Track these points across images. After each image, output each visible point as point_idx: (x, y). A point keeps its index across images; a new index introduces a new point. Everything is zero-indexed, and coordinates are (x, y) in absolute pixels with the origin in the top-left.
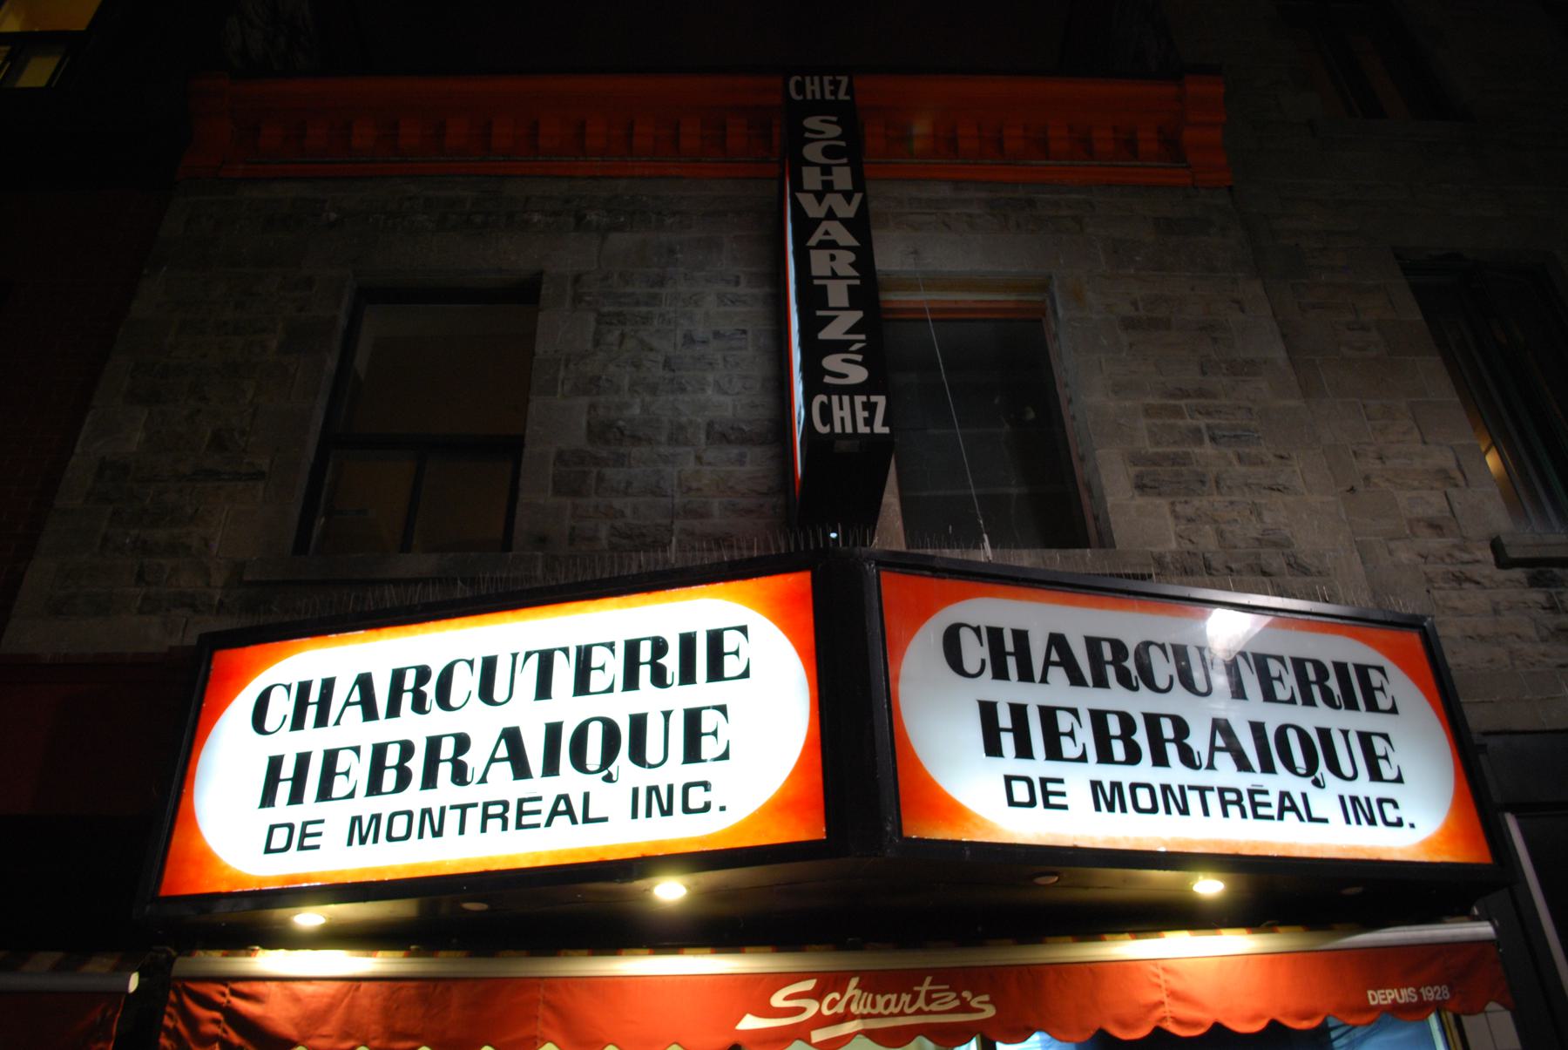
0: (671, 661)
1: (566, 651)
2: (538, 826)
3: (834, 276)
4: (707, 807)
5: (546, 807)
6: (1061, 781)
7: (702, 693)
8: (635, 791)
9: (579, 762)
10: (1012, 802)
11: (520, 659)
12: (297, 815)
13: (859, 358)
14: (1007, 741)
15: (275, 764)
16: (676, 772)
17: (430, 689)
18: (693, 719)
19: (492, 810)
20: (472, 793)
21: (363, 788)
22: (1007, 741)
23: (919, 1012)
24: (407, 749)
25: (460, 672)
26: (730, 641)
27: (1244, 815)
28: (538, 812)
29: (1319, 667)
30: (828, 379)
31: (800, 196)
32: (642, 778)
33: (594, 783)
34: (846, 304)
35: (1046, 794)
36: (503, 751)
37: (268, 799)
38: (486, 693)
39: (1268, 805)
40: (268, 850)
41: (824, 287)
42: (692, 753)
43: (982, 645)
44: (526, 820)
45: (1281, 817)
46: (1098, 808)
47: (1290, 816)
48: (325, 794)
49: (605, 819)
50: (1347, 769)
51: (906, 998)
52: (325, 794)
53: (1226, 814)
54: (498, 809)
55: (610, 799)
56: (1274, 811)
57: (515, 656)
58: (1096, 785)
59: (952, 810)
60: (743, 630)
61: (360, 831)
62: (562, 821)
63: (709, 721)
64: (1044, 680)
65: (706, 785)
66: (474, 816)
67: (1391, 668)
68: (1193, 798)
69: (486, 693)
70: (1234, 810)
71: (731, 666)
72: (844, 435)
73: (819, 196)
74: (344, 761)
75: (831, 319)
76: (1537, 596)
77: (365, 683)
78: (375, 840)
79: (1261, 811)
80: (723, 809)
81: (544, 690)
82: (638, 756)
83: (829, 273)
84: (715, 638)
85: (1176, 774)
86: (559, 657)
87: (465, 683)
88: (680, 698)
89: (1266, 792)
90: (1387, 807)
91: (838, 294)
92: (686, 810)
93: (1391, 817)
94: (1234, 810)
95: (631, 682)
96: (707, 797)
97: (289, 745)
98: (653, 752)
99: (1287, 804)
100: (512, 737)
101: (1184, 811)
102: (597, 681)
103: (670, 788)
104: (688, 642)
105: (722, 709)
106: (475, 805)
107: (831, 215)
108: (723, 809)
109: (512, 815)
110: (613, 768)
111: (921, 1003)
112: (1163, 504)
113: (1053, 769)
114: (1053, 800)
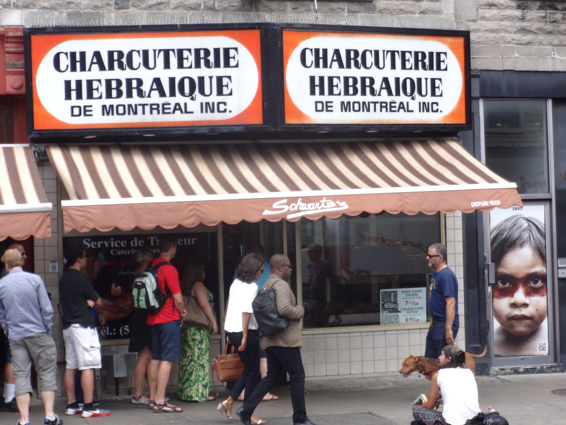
0: (211, 58)
1: (173, 50)
2: (170, 113)
4: (225, 111)
5: (172, 106)
6: (332, 102)
7: (222, 71)
8: (202, 104)
12: (82, 103)
14: (317, 89)
16: (214, 98)
17: (124, 60)
18: (220, 79)
21: (104, 95)
22: (317, 89)
24: (119, 82)
25: (135, 54)
26: (232, 53)
27: (387, 111)
28: (170, 109)
29: (424, 54)
32: (205, 100)
33: (187, 100)
35: (327, 107)
36: (155, 87)
37: (68, 97)
38: (146, 64)
39: (395, 107)
40: (73, 115)
42: (220, 92)
43: (312, 55)
44: (166, 111)
45: (398, 111)
46: (342, 111)
47: (402, 110)
48: (90, 96)
49: (192, 112)
50: (424, 93)
53: (381, 111)
54: (155, 107)
55: (194, 106)
56: (396, 109)
57: (155, 51)
58: (342, 103)
59: (299, 113)
60: (236, 49)
62: (178, 112)
63: (225, 81)
65: (225, 104)
66: (147, 108)
68: (372, 106)
69: (146, 64)
70: (384, 109)
71: (232, 62)
74: (95, 85)
76: (518, 13)
77: (97, 54)
78: (113, 114)
79: (393, 109)
80: (230, 112)
81: (167, 65)
82: (202, 92)
84: (227, 51)
85: (368, 98)
86: (171, 53)
87: (137, 60)
88: (216, 72)
89: (395, 103)
90: (435, 106)
92: (219, 111)
93: (435, 109)
94: (384, 109)
95: (198, 65)
96: (225, 107)
97: (73, 77)
98: (207, 91)
100: (157, 81)
101: (368, 110)
102: (186, 64)
103: (213, 103)
104: (217, 51)
105: (229, 77)
106: (147, 105)
108: (230, 112)
109: (161, 109)
110: (194, 95)
113: (331, 98)
114: (329, 109)
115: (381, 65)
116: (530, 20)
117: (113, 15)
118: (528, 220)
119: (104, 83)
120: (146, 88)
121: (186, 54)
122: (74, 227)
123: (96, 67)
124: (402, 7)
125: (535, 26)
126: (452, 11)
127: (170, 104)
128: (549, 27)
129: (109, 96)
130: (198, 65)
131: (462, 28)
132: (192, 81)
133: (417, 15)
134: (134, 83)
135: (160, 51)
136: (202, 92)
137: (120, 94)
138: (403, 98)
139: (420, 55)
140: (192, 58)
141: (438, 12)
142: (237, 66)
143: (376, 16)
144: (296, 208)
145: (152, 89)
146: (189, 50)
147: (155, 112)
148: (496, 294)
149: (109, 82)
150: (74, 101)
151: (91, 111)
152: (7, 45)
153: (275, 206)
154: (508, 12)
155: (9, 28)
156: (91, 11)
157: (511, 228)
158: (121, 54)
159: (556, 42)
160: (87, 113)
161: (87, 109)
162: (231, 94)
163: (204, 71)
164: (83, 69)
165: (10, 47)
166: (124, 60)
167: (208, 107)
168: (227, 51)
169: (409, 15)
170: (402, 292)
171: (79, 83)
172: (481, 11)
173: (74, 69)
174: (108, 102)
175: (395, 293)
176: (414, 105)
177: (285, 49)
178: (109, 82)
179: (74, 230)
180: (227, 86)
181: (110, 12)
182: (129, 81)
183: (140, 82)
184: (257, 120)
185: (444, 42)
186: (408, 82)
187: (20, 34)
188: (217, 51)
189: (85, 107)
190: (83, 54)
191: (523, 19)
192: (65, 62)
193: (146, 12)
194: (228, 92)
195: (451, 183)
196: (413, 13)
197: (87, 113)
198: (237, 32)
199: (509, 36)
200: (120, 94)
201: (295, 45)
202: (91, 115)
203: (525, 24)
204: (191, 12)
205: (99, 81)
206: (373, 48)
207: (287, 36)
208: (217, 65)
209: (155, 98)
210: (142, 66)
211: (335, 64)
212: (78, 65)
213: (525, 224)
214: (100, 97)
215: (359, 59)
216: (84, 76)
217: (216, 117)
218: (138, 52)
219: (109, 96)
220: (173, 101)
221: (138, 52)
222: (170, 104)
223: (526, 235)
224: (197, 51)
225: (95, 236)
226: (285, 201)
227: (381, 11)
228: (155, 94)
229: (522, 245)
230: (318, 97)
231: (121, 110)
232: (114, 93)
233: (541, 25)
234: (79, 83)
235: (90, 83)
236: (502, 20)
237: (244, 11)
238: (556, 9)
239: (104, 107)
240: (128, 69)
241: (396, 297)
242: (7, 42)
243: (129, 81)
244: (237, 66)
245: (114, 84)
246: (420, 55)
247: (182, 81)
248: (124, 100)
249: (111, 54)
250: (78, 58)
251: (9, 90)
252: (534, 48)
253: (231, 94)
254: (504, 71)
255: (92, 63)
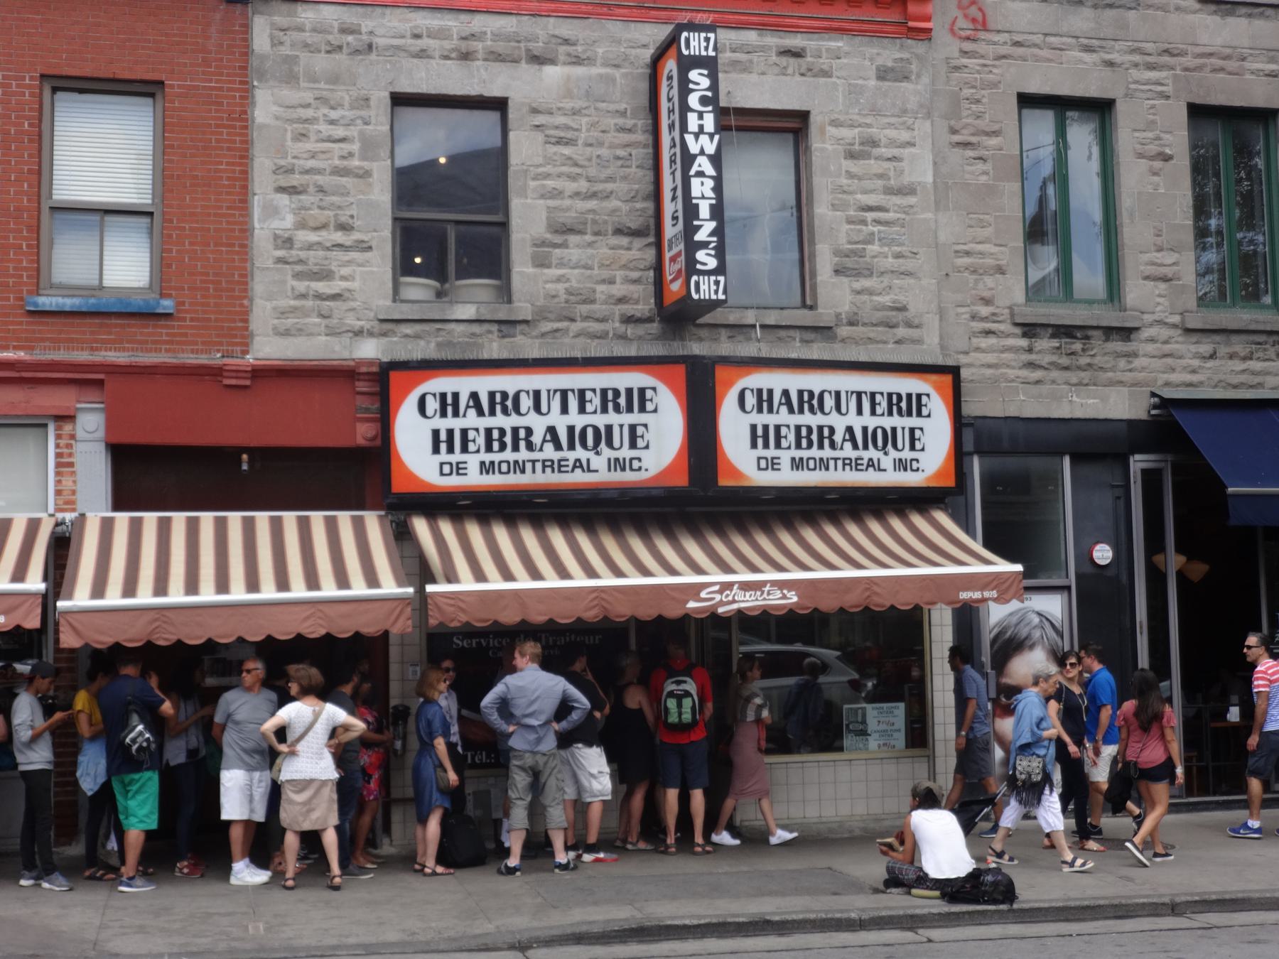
0: (622, 401)
1: (573, 391)
2: (567, 472)
3: (703, 197)
4: (640, 469)
5: (571, 463)
6: (779, 458)
8: (609, 460)
9: (584, 445)
10: (759, 469)
11: (552, 393)
13: (713, 252)
14: (760, 441)
15: (436, 433)
16: (626, 453)
17: (509, 403)
18: (633, 428)
19: (547, 463)
20: (536, 455)
21: (483, 449)
22: (760, 441)
23: (765, 599)
25: (523, 396)
26: (649, 394)
28: (567, 466)
29: (899, 396)
30: (699, 267)
31: (686, 136)
33: (591, 455)
34: (708, 217)
35: (773, 464)
36: (548, 437)
37: (436, 450)
40: (442, 474)
41: (697, 205)
42: (633, 445)
44: (563, 469)
45: (867, 469)
46: (792, 469)
47: (871, 469)
48: (465, 449)
49: (597, 471)
50: (900, 446)
51: (759, 593)
52: (465, 449)
53: (844, 469)
54: (549, 463)
55: (599, 462)
56: (864, 467)
57: (549, 391)
58: (793, 459)
59: (736, 473)
60: (654, 389)
61: (486, 468)
62: (578, 471)
63: (640, 430)
64: (778, 412)
65: (640, 460)
66: (539, 466)
67: (934, 395)
68: (832, 463)
70: (847, 468)
71: (650, 406)
72: (705, 299)
73: (697, 136)
74: (471, 435)
75: (699, 227)
76: (1024, 343)
77: (474, 396)
78: (494, 473)
79: (859, 467)
80: (646, 470)
81: (565, 410)
82: (610, 444)
83: (700, 195)
84: (642, 391)
85: (827, 453)
86: (570, 394)
87: (526, 403)
88: (628, 419)
90: (914, 463)
91: (704, 211)
92: (631, 469)
93: (914, 467)
94: (847, 468)
97: (443, 424)
98: (616, 443)
99: (871, 463)
100: (552, 430)
101: (827, 469)
102: (589, 408)
103: (624, 459)
105: (645, 426)
107: (702, 152)
108: (646, 470)
109: (556, 466)
111: (765, 595)
112: (845, 280)
114: (775, 467)
115: (844, 410)
116: (1040, 352)
117: (495, 345)
118: (1039, 614)
119: (482, 432)
120: (537, 439)
121: (589, 395)
122: (441, 619)
123: (472, 413)
124: (872, 335)
125: (1047, 359)
126: (936, 340)
127: (567, 460)
128: (1065, 361)
129: (489, 449)
130: (604, 410)
131: (950, 362)
132: (596, 430)
133: (891, 346)
134: (522, 434)
135: (555, 391)
136: (610, 444)
137: (503, 447)
138: (872, 453)
139: (895, 397)
140: (597, 401)
141: (918, 341)
142: (655, 411)
143: (837, 346)
144: (730, 598)
145: (544, 441)
146: (594, 391)
147: (548, 470)
148: (998, 712)
149: (489, 431)
150: (444, 456)
151: (466, 468)
152: (357, 383)
153: (703, 595)
154: (1011, 342)
155: (362, 362)
156: (467, 340)
157: (1017, 625)
158: (505, 395)
159: (1074, 380)
160: (461, 471)
161: (461, 466)
162: (647, 447)
163: (612, 418)
164: (456, 414)
165: (362, 386)
166: (509, 403)
167: (617, 464)
168: (642, 391)
169: (880, 346)
170: (873, 709)
171: (450, 433)
172: (974, 340)
173: (444, 414)
174: (488, 457)
175: (864, 709)
176: (887, 462)
177: (718, 388)
178: (489, 431)
179: (441, 624)
180: (642, 437)
181: (491, 341)
182: (515, 431)
183: (529, 431)
184: (682, 481)
185: (926, 380)
186: (879, 432)
187: (375, 369)
188: (629, 391)
189: (458, 463)
190: (456, 396)
191: (1030, 350)
192: (432, 405)
193: (537, 341)
194: (644, 444)
195: (832, 567)
196: (885, 342)
197: (461, 471)
198: (656, 368)
199: (1012, 373)
200: (503, 447)
201: (730, 384)
202: (466, 474)
203: (1033, 357)
204: (597, 341)
205: (477, 430)
206: (833, 388)
207: (721, 373)
208: (630, 409)
209: (549, 452)
210: (532, 411)
211: (784, 409)
212: (450, 409)
213: (1036, 620)
214: (478, 451)
215: (815, 402)
216: (456, 424)
217: (628, 477)
218: (528, 392)
219: (489, 449)
220: (572, 456)
221: (528, 392)
222: (567, 460)
223: (1037, 634)
224: (604, 392)
225: (469, 632)
226: (716, 588)
227: (843, 341)
228: (549, 447)
229: (1032, 647)
230: (760, 452)
231: (504, 467)
232: (496, 445)
233: (1054, 358)
234: (450, 433)
235: (464, 432)
236: (1002, 352)
237: (666, 339)
238: (1076, 338)
239: (482, 463)
240: (513, 414)
241: (864, 715)
242: (358, 380)
243: (515, 431)
244: (655, 411)
245: (496, 434)
246: (895, 397)
247: (584, 431)
248: (508, 455)
249: (492, 395)
250: (449, 400)
251: (360, 441)
252: (1045, 389)
253: (647, 447)
254: (1006, 418)
255: (468, 407)
